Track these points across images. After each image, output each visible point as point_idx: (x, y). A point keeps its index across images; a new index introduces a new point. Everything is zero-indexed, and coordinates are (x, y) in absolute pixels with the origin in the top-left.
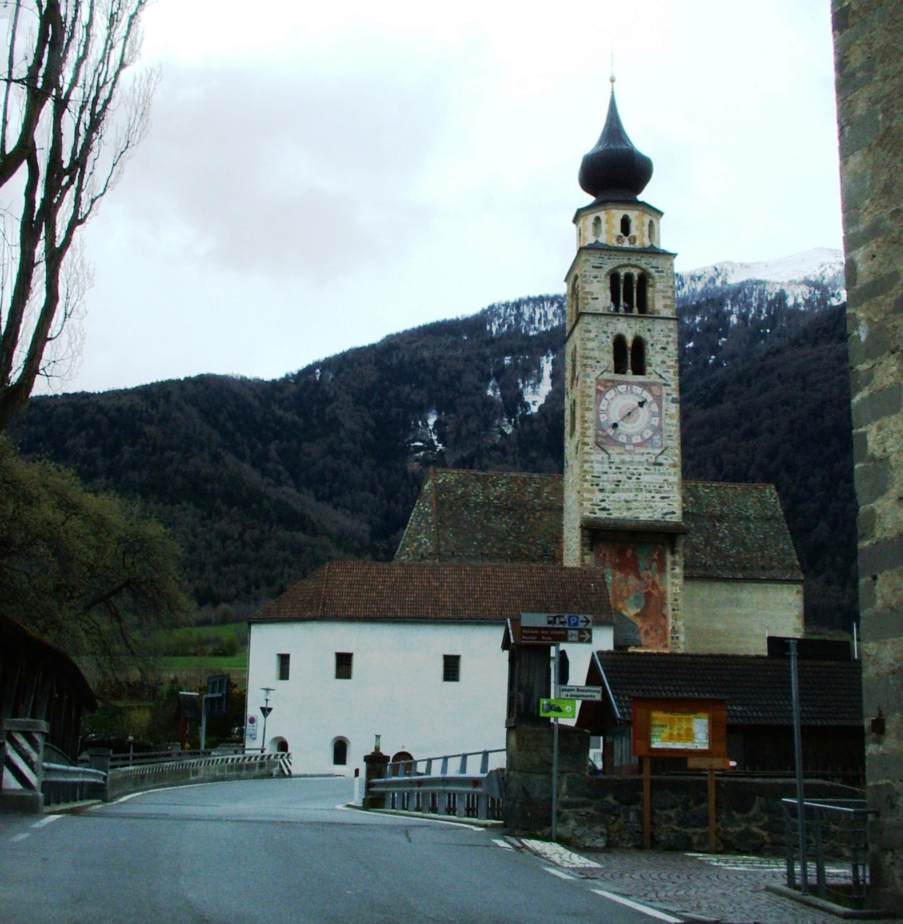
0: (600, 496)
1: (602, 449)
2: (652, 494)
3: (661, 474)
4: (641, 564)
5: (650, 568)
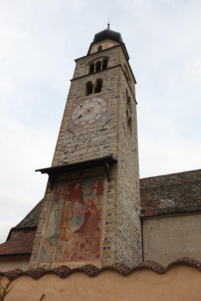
0: (64, 156)
1: (70, 131)
2: (98, 147)
3: (105, 135)
4: (84, 192)
5: (91, 194)
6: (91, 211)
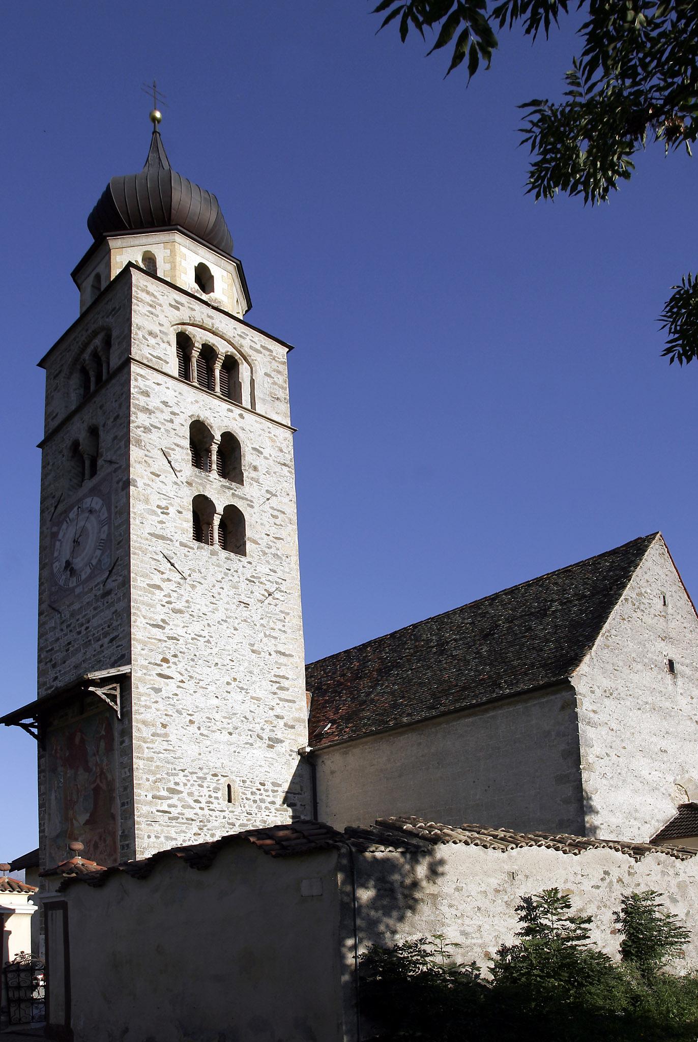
6: (101, 785)
